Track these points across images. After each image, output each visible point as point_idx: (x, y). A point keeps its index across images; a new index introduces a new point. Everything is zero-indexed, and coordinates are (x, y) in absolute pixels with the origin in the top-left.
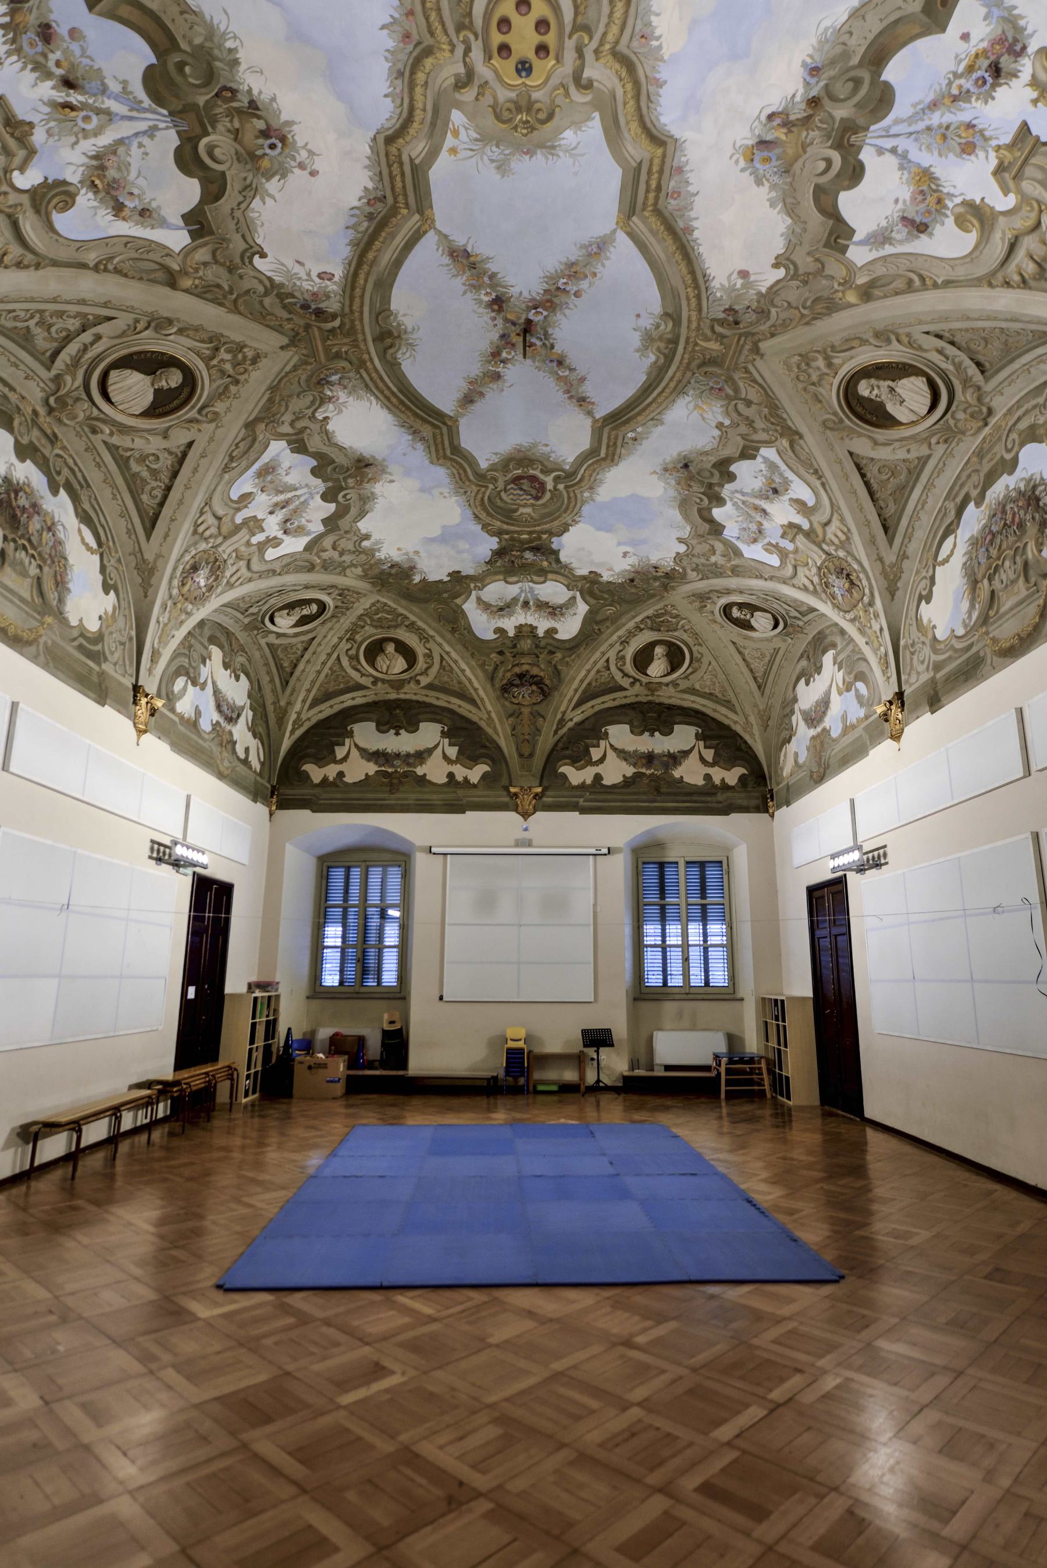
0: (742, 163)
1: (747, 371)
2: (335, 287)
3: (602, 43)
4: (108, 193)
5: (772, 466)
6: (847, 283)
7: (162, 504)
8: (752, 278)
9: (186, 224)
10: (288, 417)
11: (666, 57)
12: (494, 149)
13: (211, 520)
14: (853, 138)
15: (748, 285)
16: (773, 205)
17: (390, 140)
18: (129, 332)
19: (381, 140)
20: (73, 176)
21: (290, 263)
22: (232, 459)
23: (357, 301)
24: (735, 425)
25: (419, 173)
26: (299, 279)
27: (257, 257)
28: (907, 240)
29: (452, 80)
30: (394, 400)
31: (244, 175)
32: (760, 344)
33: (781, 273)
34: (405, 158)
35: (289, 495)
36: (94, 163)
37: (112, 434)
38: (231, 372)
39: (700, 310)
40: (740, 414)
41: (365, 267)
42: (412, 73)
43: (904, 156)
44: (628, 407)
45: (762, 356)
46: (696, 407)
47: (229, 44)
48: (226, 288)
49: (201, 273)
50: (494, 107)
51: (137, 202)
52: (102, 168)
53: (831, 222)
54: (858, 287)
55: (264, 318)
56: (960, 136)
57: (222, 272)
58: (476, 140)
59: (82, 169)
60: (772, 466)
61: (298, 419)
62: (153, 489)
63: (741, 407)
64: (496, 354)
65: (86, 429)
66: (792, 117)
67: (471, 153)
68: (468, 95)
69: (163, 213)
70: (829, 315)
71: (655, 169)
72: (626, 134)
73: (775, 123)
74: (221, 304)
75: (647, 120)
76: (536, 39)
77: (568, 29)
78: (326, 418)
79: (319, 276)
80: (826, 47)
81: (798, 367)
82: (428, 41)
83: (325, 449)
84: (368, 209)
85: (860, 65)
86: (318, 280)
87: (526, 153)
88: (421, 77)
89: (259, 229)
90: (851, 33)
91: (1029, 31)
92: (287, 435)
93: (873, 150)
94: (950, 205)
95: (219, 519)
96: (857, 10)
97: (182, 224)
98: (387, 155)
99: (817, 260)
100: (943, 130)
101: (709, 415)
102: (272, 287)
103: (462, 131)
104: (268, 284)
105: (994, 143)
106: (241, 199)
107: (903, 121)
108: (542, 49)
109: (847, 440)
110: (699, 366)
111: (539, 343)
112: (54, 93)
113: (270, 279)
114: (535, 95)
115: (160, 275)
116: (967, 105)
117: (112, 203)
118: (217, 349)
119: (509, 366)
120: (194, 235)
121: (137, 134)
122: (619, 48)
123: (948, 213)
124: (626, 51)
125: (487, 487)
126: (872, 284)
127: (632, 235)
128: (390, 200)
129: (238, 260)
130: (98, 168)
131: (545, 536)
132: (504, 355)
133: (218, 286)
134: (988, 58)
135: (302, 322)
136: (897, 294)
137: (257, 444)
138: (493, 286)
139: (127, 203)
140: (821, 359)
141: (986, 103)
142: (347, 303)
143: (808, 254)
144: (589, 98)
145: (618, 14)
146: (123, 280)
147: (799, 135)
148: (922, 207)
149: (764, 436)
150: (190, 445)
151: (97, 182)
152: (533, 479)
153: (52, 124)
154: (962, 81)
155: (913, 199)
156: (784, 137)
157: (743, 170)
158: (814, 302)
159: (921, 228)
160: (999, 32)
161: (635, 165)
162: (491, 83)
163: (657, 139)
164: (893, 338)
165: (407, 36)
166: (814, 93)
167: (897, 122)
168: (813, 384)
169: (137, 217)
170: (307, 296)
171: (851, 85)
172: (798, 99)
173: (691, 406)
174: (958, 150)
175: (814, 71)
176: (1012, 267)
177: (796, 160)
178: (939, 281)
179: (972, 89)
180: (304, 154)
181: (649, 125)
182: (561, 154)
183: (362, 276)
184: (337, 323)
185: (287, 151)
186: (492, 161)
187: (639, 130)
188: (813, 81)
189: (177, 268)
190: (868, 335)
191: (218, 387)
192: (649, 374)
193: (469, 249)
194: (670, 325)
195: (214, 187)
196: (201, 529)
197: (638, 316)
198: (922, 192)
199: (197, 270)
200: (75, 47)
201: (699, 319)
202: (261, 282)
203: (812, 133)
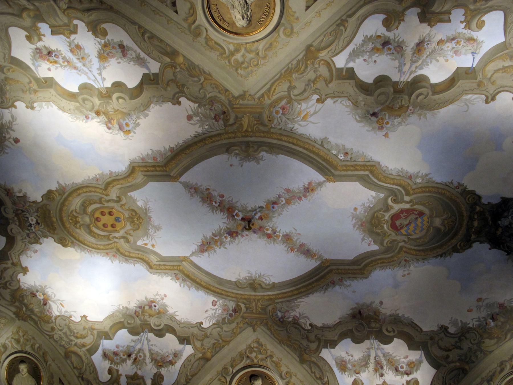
0: (132, 134)
1: (263, 96)
3: (104, 194)
5: (354, 55)
6: (173, 66)
8: (190, 113)
10: (305, 343)
11: (101, 172)
12: (150, 231)
14: (104, 93)
15: (196, 114)
16: (147, 115)
17: (151, 267)
19: (151, 270)
20: (155, 370)
21: (206, 315)
22: (321, 379)
23: (229, 294)
24: (316, 91)
25: (163, 259)
26: (215, 314)
28: (132, 50)
29: (127, 243)
30: (302, 290)
32: (236, 96)
33: (183, 100)
34: (158, 263)
35: (372, 360)
36: (154, 362)
38: (264, 356)
39: (220, 135)
40: (305, 90)
41: (210, 287)
42: (126, 256)
43: (99, 69)
44: (309, 161)
45: (245, 92)
46: (304, 118)
47: (121, 308)
49: (206, 348)
50: (134, 231)
51: (171, 356)
52: (156, 360)
53: (145, 86)
54: (172, 59)
55: (234, 333)
56: (78, 53)
57: (206, 340)
58: (147, 237)
60: (354, 55)
61: (307, 338)
63: (296, 92)
64: (269, 236)
66: (106, 120)
67: (153, 240)
68: (131, 238)
69: (177, 350)
70: (198, 66)
71: (145, 169)
72: (134, 182)
73: (111, 126)
74: (223, 346)
75: (126, 175)
76: (107, 217)
77: (102, 205)
78: (311, 325)
80: (78, 116)
81: (248, 67)
82: (114, 250)
84: (181, 280)
85: (78, 101)
86: (216, 307)
87: (150, 220)
88: (126, 253)
89: (189, 321)
90: (70, 109)
91: (31, 51)
92: (318, 347)
93: (105, 83)
94: (103, 41)
96: (62, 110)
97: (183, 345)
98: (157, 269)
99: (168, 85)
100: (81, 60)
101: (312, 110)
103: (145, 242)
105: (68, 40)
107: (88, 77)
108: (110, 214)
109: (297, 15)
110: (265, 126)
111: (259, 214)
112: (131, 361)
113: (214, 324)
114: (127, 216)
115: (202, 362)
116: (66, 56)
117: (168, 364)
118: (248, 357)
119: (278, 230)
120: (189, 343)
122: (103, 188)
123: (106, 40)
124: (103, 186)
125: (401, 248)
126: (166, 54)
127: (181, 175)
128: (177, 272)
129: (203, 333)
131: (478, 209)
132: (269, 232)
133: (214, 344)
134: (49, 59)
135: (240, 319)
136: (161, 41)
137: (319, 363)
138: (220, 235)
139: (170, 359)
140: (233, 58)
141: (60, 51)
142: (231, 298)
143: (166, 90)
144: (123, 197)
145: (93, 189)
146: (197, 376)
147: (112, 114)
148: (113, 51)
149: (323, 70)
151: (160, 364)
152: (395, 217)
153: (138, 367)
154: (61, 63)
155: (113, 57)
156: (115, 121)
157: (135, 133)
158: (194, 77)
159: (122, 47)
160: (40, 59)
161: (146, 177)
162: (125, 231)
163: (133, 169)
164: (193, 26)
165: (114, 256)
166: (94, 115)
167: (89, 78)
168: (258, 54)
169: (176, 359)
171: (86, 102)
172: (99, 120)
173: (303, 123)
174: (82, 51)
175: (87, 117)
176: (93, 5)
177: (123, 112)
178: (137, 27)
179: (61, 58)
180: (157, 297)
181: (128, 174)
182: (148, 206)
183: (215, 289)
184: (243, 306)
186: (155, 232)
187: (131, 178)
188: (90, 117)
190: (202, 39)
192: (278, 154)
193: (200, 244)
194: (235, 148)
197: (231, 165)
198: (108, 55)
199: (204, 349)
200: (121, 349)
201: (227, 133)
202: (215, 328)
203: (109, 110)
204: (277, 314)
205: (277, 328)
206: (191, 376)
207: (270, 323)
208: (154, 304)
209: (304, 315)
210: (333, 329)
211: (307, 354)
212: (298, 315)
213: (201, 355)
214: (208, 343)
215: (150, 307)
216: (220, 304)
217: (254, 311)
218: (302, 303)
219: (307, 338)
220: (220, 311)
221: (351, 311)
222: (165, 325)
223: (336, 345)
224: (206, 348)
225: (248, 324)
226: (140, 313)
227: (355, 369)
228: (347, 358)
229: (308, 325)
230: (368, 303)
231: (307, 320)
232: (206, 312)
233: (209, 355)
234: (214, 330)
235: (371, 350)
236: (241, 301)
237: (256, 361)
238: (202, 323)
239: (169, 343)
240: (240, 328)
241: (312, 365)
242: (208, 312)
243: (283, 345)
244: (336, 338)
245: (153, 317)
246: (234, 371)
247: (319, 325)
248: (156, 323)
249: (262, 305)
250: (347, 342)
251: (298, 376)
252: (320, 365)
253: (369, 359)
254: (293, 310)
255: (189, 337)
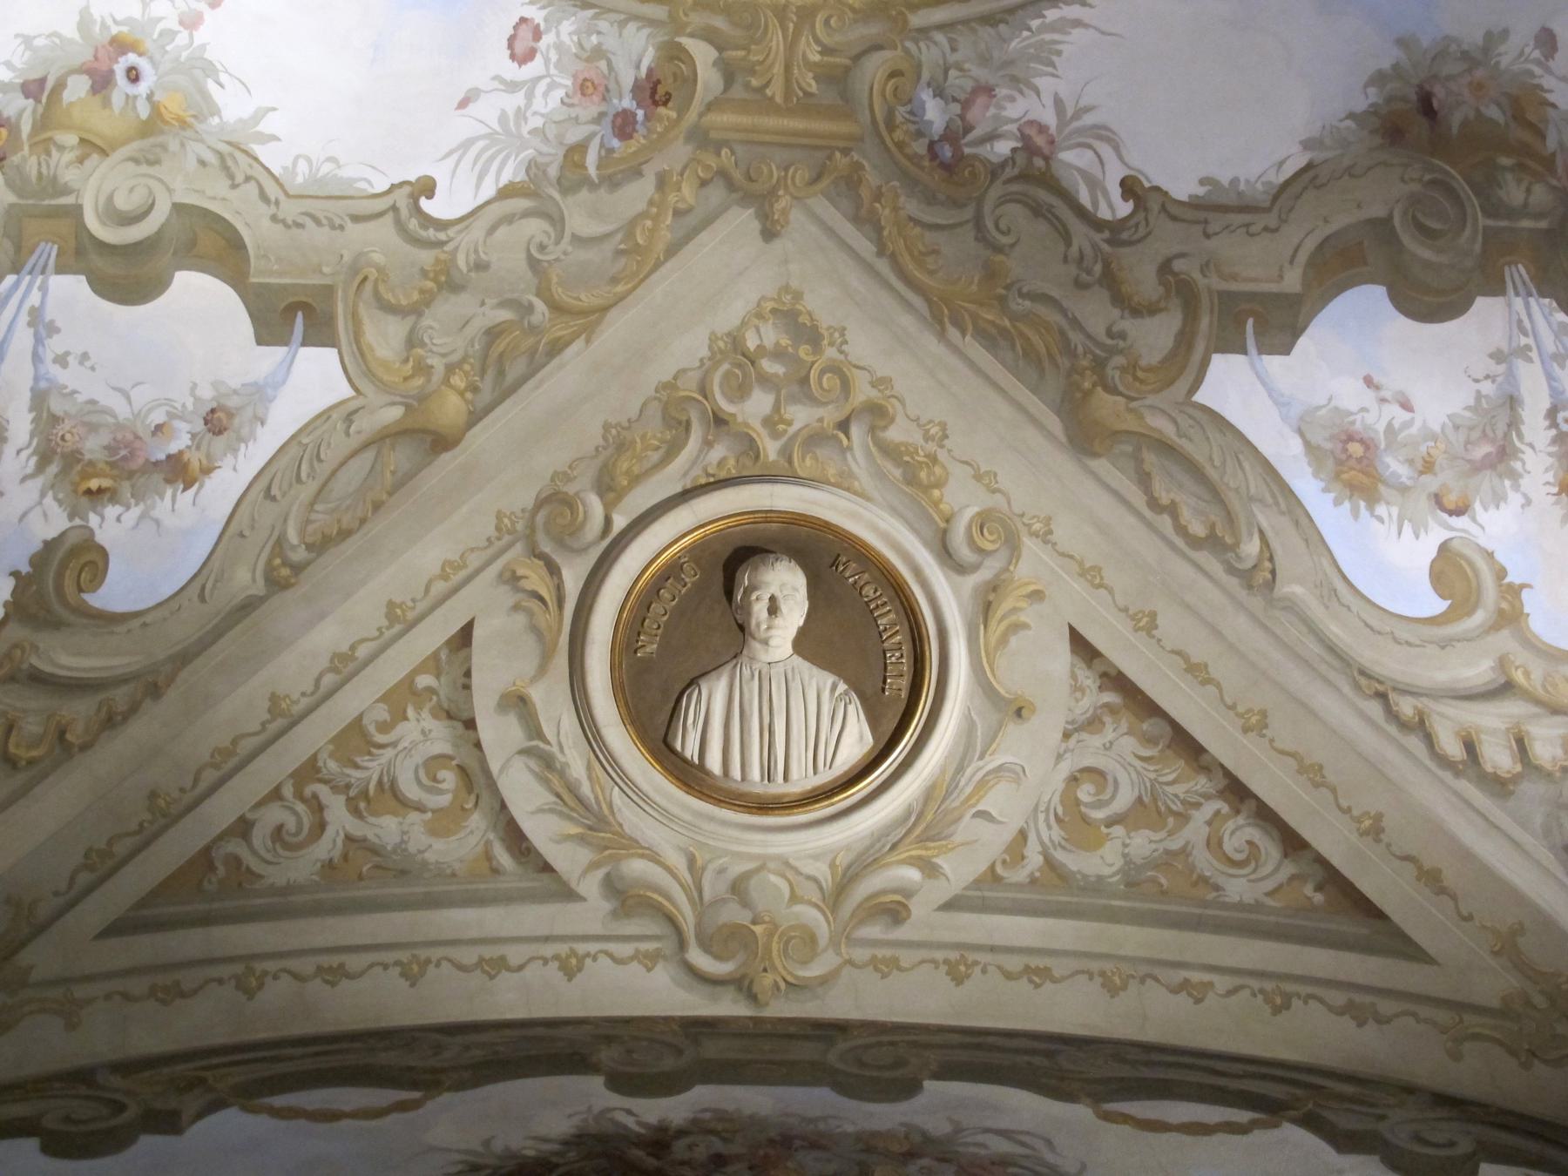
2: (567, 27)
4: (131, 475)
7: (1292, 843)
9: (284, 341)
10: (1096, 313)
13: (1491, 720)
18: (544, 619)
21: (464, 126)
22: (1213, 542)
26: (521, 115)
27: (424, 203)
31: (191, 163)
37: (930, 869)
38: (830, 415)
48: (505, 315)
49: (438, 363)
55: (636, 249)
57: (448, 308)
59: (49, 500)
61: (1110, 281)
62: (1214, 844)
65: (874, 931)
69: (235, 383)
74: (556, 348)
78: (1130, 187)
79: (522, 57)
83: (1305, 232)
86: (535, 67)
89: (346, 173)
92: (1185, 340)
95: (1504, 689)
97: (279, 352)
102: (528, 194)
104: (523, 204)
106: (252, 188)
113: (505, 193)
115: (399, 457)
117: (157, 478)
118: (720, 420)
120: (320, 332)
121: (36, 358)
129: (426, 257)
130: (65, 470)
133: (493, 334)
135: (679, 152)
137: (1195, 449)
139: (173, 448)
150: (1081, 646)
169: (220, 442)
170: (592, 108)
184: (702, 54)
185: (148, 45)
189: (397, 412)
191: (881, 475)
195: (213, 244)
196: (1498, 758)
199: (423, 369)
202: (509, 219)
204: (916, 113)
205: (911, 207)
206: (309, 547)
207: (872, 178)
208: (132, 58)
209: (1088, 120)
210: (1271, 220)
211: (1113, 390)
212: (1049, 118)
213: (395, 413)
214: (454, 327)
215: (101, 83)
216: (559, 46)
217: (776, 90)
218: (1077, 32)
219: (1110, 281)
220: (559, 93)
221: (1374, 96)
222: (178, 208)
223: (1296, 331)
224: (438, 363)
225: (731, 185)
226: (26, 128)
227: (1432, 483)
228: (1377, 418)
229: (1115, 192)
230: (1473, 36)
231: (1106, 151)
232: (464, 103)
233: (450, 408)
234: (501, 232)
235: (1521, 367)
236: (697, 19)
237: (771, 449)
238: (427, 187)
239: (196, 329)
240: (677, 213)
241: (1150, 459)
242: (472, 109)
243: (953, 333)
244: (1292, 281)
245: (104, 153)
246: (620, 522)
247: (1182, 188)
248: (123, 203)
249: (826, 51)
250: (1366, 302)
251: (1060, 534)
252: (1199, 457)
253: (1514, 423)
254: (1015, 81)
255: (328, 291)
